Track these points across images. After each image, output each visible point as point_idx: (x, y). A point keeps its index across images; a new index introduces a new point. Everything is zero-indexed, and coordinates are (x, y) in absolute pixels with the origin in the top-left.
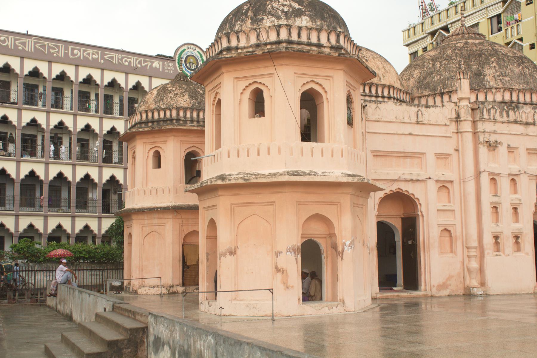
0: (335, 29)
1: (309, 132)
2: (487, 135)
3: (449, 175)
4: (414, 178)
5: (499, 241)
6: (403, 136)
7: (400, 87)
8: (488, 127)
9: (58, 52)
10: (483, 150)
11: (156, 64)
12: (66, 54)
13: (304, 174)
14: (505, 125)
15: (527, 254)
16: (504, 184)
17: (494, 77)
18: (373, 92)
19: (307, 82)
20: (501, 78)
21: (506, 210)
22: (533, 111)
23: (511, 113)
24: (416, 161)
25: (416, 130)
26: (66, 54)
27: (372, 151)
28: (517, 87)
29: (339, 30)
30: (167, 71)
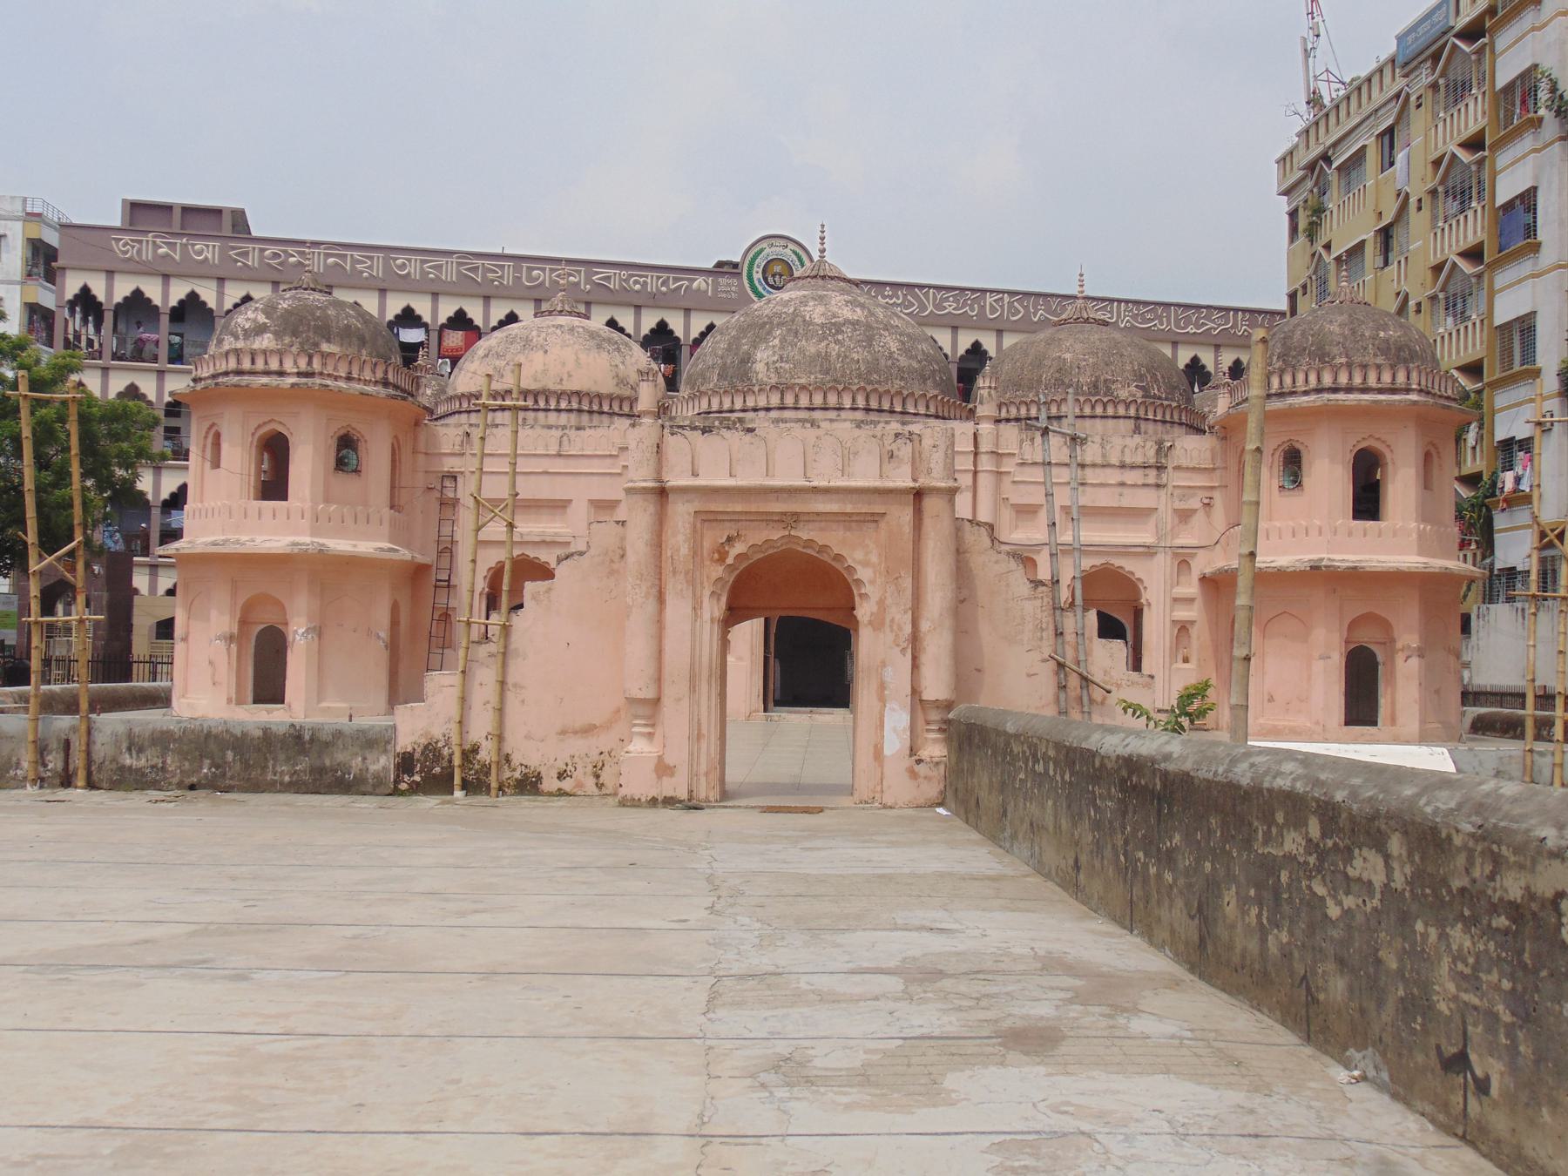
0: (316, 345)
1: (274, 487)
4: (548, 539)
6: (533, 478)
11: (699, 283)
13: (237, 542)
15: (740, 659)
18: (542, 404)
28: (803, 381)
29: (325, 347)
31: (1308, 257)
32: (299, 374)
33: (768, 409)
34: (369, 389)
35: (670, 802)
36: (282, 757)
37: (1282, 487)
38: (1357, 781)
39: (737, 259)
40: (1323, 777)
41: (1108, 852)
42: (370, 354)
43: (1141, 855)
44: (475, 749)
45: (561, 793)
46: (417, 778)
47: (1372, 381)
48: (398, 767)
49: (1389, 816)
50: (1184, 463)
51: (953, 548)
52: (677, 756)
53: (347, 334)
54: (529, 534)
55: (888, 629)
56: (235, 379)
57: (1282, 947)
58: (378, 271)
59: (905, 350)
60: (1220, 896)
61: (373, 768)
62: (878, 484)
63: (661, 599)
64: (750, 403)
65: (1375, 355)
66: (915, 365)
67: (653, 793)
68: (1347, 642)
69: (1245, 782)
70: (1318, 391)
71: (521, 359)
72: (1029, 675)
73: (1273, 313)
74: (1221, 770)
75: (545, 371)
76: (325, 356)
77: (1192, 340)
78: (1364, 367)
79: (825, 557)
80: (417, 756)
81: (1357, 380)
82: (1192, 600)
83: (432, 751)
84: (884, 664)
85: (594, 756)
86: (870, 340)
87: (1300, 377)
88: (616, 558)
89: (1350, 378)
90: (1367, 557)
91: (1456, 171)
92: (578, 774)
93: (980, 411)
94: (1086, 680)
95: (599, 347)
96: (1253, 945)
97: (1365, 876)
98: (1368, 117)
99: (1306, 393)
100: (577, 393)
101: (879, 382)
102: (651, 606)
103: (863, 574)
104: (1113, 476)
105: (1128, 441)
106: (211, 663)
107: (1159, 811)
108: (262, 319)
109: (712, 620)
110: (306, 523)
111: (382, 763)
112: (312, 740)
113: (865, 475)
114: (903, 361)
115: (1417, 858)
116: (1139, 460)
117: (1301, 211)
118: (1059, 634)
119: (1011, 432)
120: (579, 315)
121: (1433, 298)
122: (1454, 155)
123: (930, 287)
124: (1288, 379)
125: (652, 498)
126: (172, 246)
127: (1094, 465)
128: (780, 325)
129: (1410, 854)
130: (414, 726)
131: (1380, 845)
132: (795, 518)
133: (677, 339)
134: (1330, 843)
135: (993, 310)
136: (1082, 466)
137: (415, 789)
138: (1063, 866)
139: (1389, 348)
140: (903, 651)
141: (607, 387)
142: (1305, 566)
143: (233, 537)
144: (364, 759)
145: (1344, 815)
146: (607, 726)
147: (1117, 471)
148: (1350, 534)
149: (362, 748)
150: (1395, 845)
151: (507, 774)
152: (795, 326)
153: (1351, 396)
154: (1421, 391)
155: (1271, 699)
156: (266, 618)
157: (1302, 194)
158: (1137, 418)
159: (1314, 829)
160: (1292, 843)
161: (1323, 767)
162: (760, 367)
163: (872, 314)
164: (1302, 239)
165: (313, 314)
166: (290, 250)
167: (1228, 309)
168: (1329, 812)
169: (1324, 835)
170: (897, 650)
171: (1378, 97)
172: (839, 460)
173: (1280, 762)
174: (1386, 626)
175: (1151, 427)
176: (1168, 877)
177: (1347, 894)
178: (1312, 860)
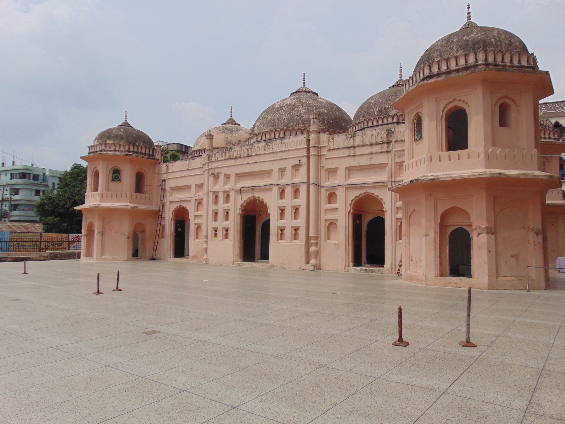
0: (106, 141)
2: (213, 170)
3: (201, 194)
5: (214, 232)
7: (226, 146)
8: (214, 165)
10: (211, 178)
14: (223, 162)
15: (230, 241)
16: (221, 197)
21: (221, 215)
23: (227, 153)
27: (171, 188)
29: (108, 142)
34: (119, 153)
47: (453, 66)
50: (400, 138)
54: (182, 198)
65: (457, 51)
68: (442, 227)
90: (448, 173)
104: (367, 150)
110: (98, 198)
114: (306, 117)
116: (379, 140)
119: (324, 137)
127: (359, 146)
136: (354, 147)
139: (467, 45)
148: (440, 161)
155: (412, 260)
162: (256, 128)
163: (300, 100)
174: (466, 214)
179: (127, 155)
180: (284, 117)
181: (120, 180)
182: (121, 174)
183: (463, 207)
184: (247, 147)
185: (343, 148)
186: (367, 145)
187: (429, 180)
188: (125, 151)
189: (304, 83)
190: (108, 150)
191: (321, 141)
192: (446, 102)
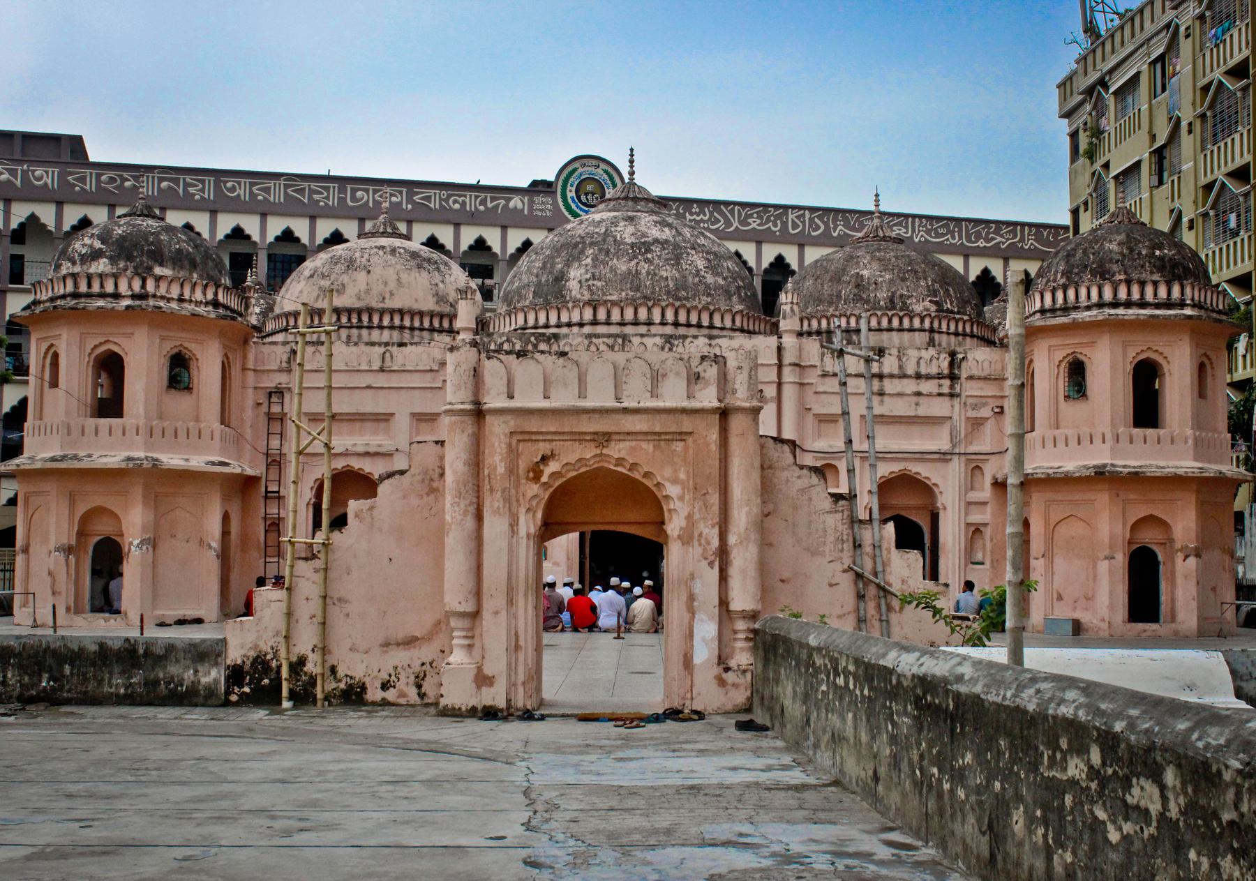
0: (150, 269)
4: (372, 450)
6: (357, 391)
7: (437, 309)
9: (327, 198)
11: (516, 202)
12: (342, 200)
13: (75, 457)
15: (556, 564)
17: (580, 282)
19: (101, 344)
20: (591, 282)
22: (586, 342)
24: (382, 425)
25: (381, 380)
26: (342, 200)
28: (614, 298)
30: (539, 213)
31: (1088, 176)
32: (134, 297)
33: (581, 325)
34: (201, 310)
35: (490, 714)
36: (117, 670)
37: (1067, 397)
38: (1134, 712)
39: (552, 178)
40: (1103, 706)
41: (904, 766)
42: (201, 277)
43: (935, 770)
44: (302, 661)
45: (385, 703)
46: (247, 689)
47: (1149, 296)
48: (227, 679)
49: (1164, 750)
50: (975, 372)
51: (757, 464)
52: (496, 665)
53: (178, 259)
55: (696, 543)
56: (72, 302)
57: (1066, 867)
58: (210, 194)
59: (713, 268)
60: (1009, 815)
61: (204, 680)
62: (686, 404)
63: (479, 517)
64: (565, 319)
65: (1152, 273)
66: (721, 282)
67: (472, 702)
68: (1129, 543)
69: (1031, 707)
70: (1100, 305)
71: (345, 278)
72: (831, 585)
73: (1057, 228)
74: (1009, 694)
75: (368, 291)
76: (158, 279)
77: (982, 253)
78: (1142, 284)
79: (636, 475)
80: (247, 668)
81: (1136, 296)
82: (985, 503)
83: (261, 664)
84: (692, 576)
85: (416, 667)
86: (678, 258)
87: (1083, 292)
88: (436, 476)
89: (1129, 294)
90: (1148, 463)
91: (1225, 95)
92: (401, 685)
93: (784, 325)
94: (884, 591)
95: (419, 267)
96: (1040, 864)
97: (1142, 803)
98: (1141, 46)
99: (1088, 308)
100: (401, 312)
101: (687, 299)
102: (470, 523)
103: (672, 490)
104: (910, 386)
105: (923, 353)
106: (50, 573)
107: (953, 730)
108: (98, 244)
109: (528, 536)
111: (213, 676)
112: (147, 653)
113: (673, 395)
114: (710, 279)
115: (1190, 790)
116: (934, 370)
117: (1081, 132)
118: (857, 546)
119: (812, 347)
120: (401, 236)
121: (1205, 215)
122: (1220, 83)
123: (735, 203)
124: (1071, 293)
125: (469, 420)
126: (13, 172)
127: (891, 376)
128: (592, 244)
129: (1184, 784)
130: (241, 641)
131: (1156, 776)
132: (605, 438)
133: (495, 254)
134: (1110, 771)
135: (795, 226)
136: (881, 377)
137: (245, 701)
138: (863, 774)
140: (711, 564)
141: (428, 304)
142: (1091, 472)
143: (70, 452)
144: (196, 671)
145: (1123, 745)
146: (429, 637)
147: (913, 381)
148: (1131, 442)
149: (194, 661)
150: (1170, 777)
151: (334, 685)
152: (605, 245)
153: (1130, 311)
154: (1194, 306)
155: (1060, 598)
156: (103, 528)
157: (1084, 115)
158: (932, 331)
159: (1096, 757)
160: (1075, 769)
161: (1104, 697)
162: (573, 285)
163: (680, 234)
164: (1082, 161)
165: (146, 240)
166: (125, 175)
167: (1015, 224)
168: (1109, 742)
169: (1104, 763)
170: (705, 563)
171: (1150, 28)
172: (649, 383)
173: (1064, 690)
175: (944, 337)
176: (961, 793)
177: (1126, 819)
178: (1094, 785)
179: (224, 317)
180: (664, 274)
181: (189, 389)
182: (194, 372)
183: (1163, 517)
184: (610, 341)
185: (856, 376)
186: (910, 377)
187: (1129, 473)
188: (207, 304)
189: (632, 173)
190: (163, 298)
191: (804, 354)
192: (1137, 349)
